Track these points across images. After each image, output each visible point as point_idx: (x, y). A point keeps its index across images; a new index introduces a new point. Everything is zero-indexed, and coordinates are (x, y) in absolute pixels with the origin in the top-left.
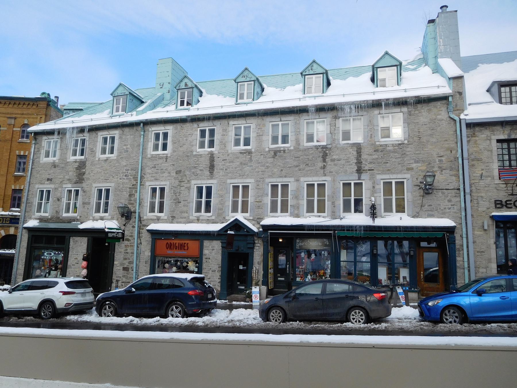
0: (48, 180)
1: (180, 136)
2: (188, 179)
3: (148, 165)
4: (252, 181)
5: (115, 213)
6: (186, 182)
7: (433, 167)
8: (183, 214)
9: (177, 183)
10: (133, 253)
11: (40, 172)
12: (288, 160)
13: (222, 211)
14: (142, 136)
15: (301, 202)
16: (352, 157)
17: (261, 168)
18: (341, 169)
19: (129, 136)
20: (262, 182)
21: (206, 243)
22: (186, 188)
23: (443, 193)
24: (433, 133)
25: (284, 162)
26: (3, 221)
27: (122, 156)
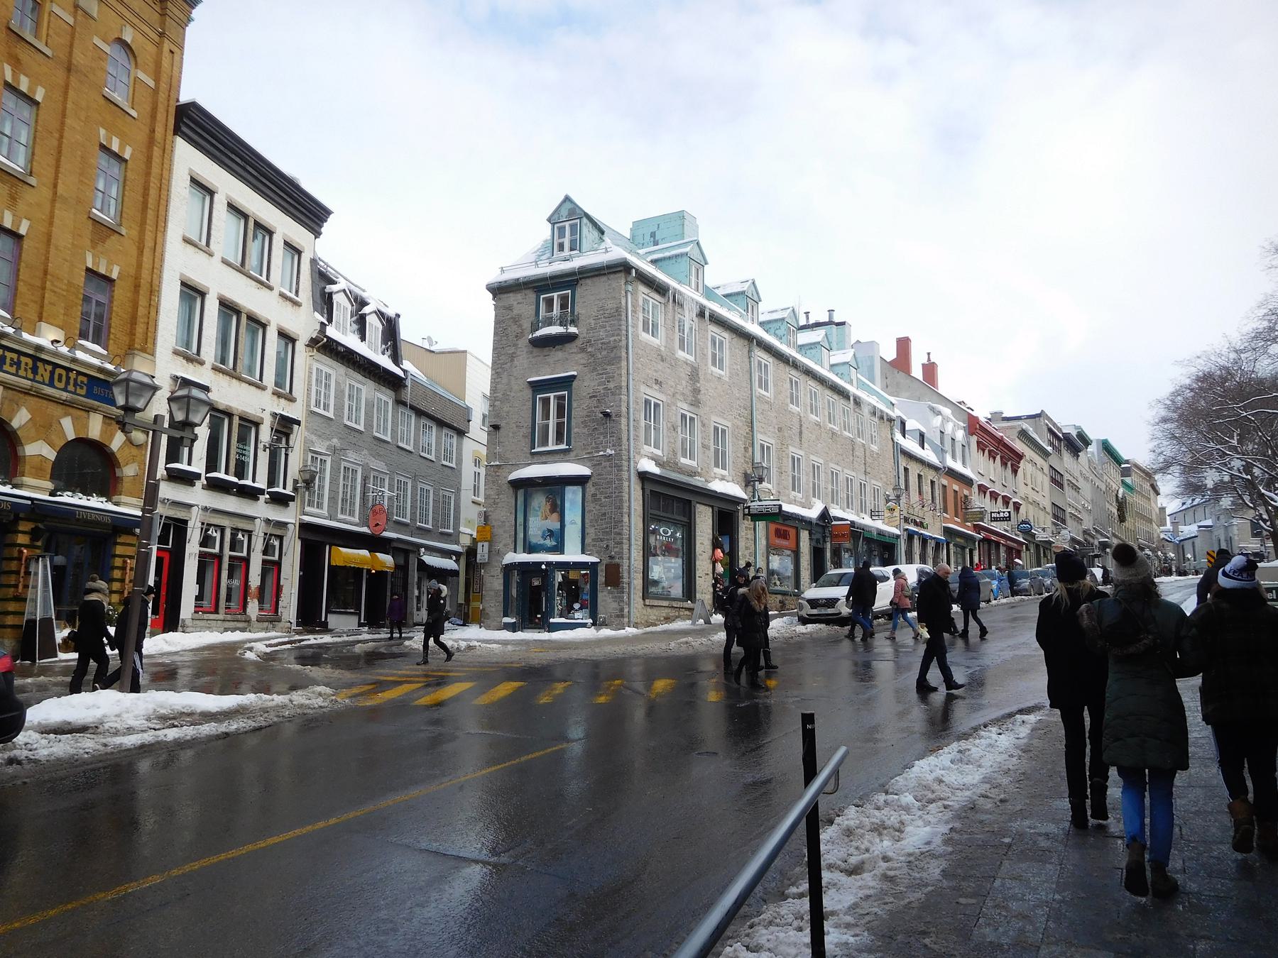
26: (67, 383)
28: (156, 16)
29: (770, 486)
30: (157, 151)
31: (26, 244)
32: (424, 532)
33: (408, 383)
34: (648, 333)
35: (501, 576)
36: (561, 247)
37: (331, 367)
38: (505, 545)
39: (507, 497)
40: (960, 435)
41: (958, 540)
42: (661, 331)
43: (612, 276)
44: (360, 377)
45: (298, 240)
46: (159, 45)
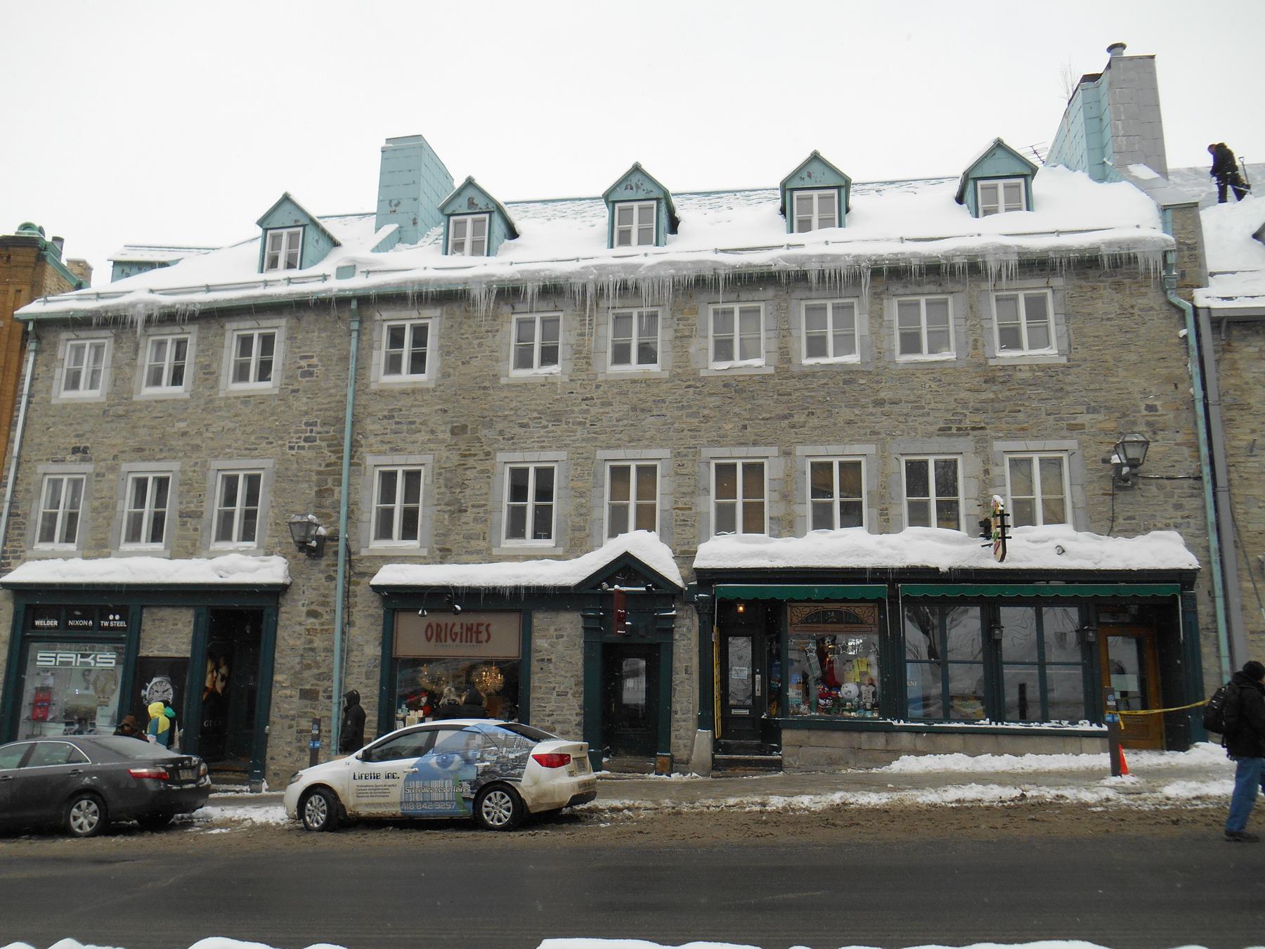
0: (76, 450)
1: (462, 334)
2: (487, 449)
3: (370, 410)
4: (665, 453)
5: (277, 540)
6: (482, 457)
7: (1134, 423)
8: (473, 542)
9: (455, 459)
10: (329, 650)
11: (51, 430)
12: (760, 402)
13: (583, 534)
14: (355, 334)
15: (797, 509)
16: (929, 396)
17: (688, 420)
18: (902, 426)
19: (316, 334)
20: (691, 457)
21: (539, 619)
22: (483, 471)
23: (1160, 488)
24: (1130, 339)
25: (749, 406)
27: (296, 386)
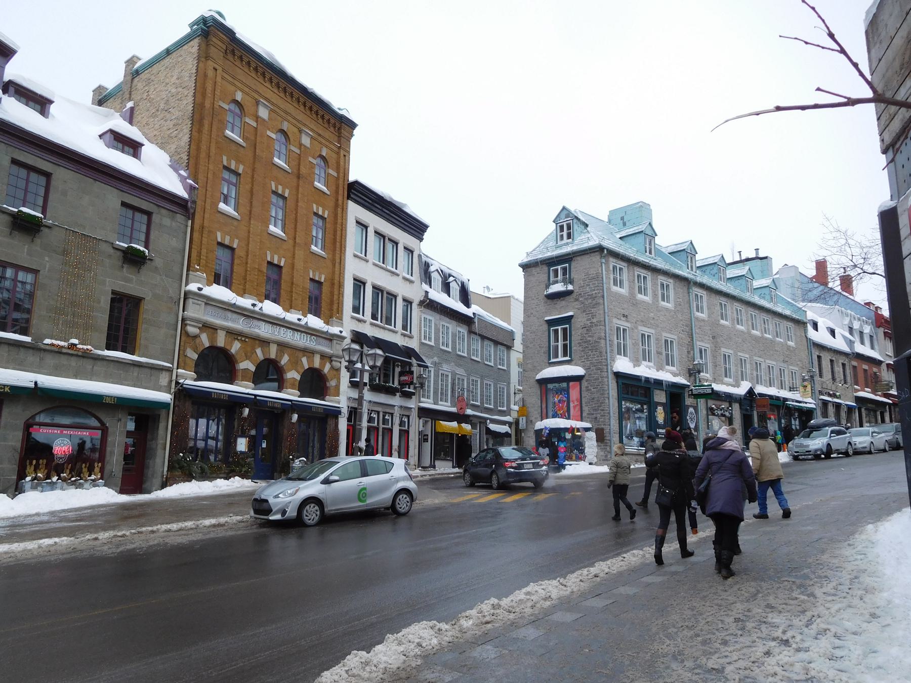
0: (624, 316)
28: (336, 138)
29: (708, 375)
30: (339, 210)
31: (284, 271)
32: (488, 410)
33: (476, 320)
34: (617, 286)
35: (534, 437)
36: (562, 236)
37: (432, 316)
38: (536, 418)
39: (536, 390)
40: (867, 329)
41: (869, 405)
42: (626, 284)
43: (592, 254)
44: (448, 320)
45: (411, 245)
46: (338, 153)
